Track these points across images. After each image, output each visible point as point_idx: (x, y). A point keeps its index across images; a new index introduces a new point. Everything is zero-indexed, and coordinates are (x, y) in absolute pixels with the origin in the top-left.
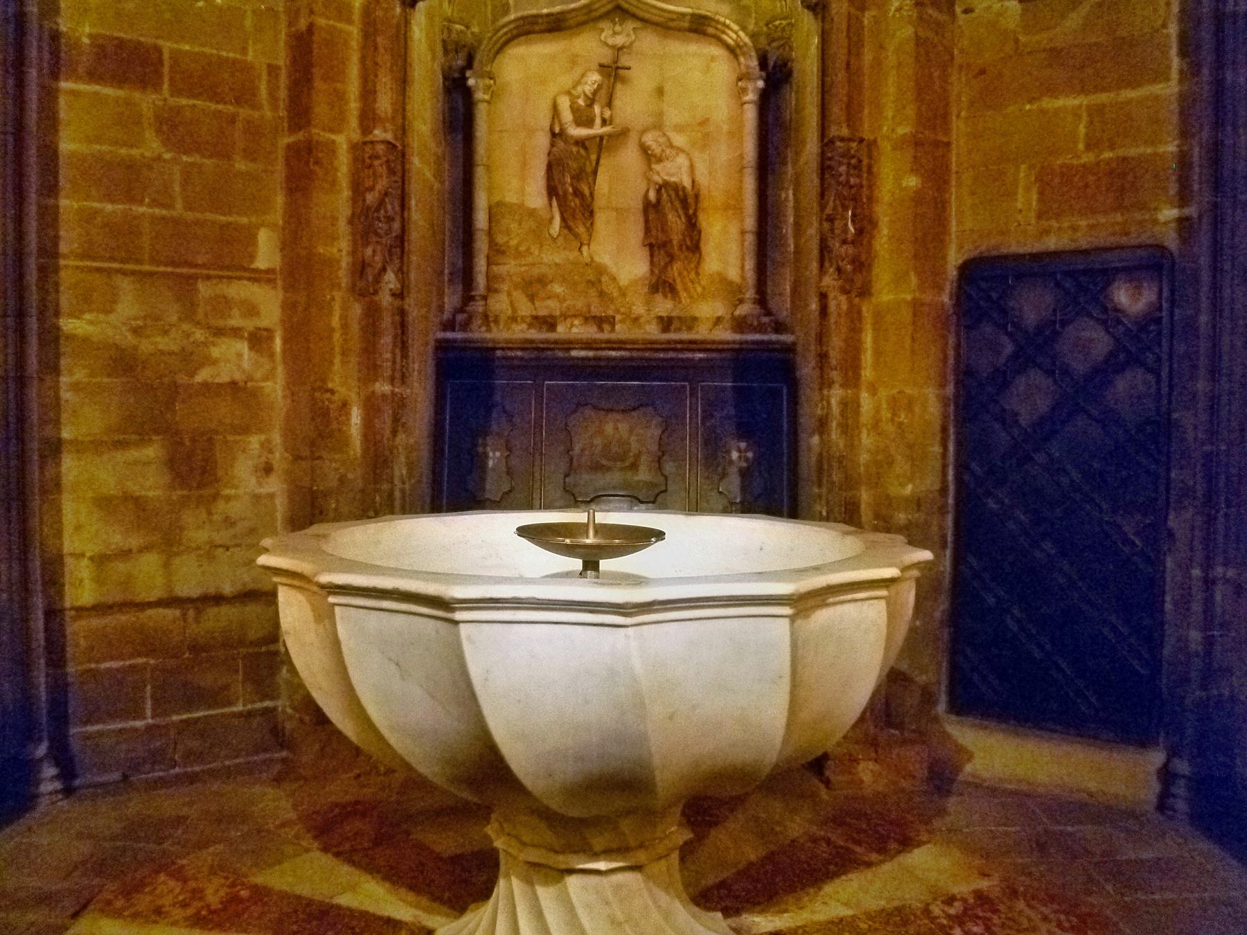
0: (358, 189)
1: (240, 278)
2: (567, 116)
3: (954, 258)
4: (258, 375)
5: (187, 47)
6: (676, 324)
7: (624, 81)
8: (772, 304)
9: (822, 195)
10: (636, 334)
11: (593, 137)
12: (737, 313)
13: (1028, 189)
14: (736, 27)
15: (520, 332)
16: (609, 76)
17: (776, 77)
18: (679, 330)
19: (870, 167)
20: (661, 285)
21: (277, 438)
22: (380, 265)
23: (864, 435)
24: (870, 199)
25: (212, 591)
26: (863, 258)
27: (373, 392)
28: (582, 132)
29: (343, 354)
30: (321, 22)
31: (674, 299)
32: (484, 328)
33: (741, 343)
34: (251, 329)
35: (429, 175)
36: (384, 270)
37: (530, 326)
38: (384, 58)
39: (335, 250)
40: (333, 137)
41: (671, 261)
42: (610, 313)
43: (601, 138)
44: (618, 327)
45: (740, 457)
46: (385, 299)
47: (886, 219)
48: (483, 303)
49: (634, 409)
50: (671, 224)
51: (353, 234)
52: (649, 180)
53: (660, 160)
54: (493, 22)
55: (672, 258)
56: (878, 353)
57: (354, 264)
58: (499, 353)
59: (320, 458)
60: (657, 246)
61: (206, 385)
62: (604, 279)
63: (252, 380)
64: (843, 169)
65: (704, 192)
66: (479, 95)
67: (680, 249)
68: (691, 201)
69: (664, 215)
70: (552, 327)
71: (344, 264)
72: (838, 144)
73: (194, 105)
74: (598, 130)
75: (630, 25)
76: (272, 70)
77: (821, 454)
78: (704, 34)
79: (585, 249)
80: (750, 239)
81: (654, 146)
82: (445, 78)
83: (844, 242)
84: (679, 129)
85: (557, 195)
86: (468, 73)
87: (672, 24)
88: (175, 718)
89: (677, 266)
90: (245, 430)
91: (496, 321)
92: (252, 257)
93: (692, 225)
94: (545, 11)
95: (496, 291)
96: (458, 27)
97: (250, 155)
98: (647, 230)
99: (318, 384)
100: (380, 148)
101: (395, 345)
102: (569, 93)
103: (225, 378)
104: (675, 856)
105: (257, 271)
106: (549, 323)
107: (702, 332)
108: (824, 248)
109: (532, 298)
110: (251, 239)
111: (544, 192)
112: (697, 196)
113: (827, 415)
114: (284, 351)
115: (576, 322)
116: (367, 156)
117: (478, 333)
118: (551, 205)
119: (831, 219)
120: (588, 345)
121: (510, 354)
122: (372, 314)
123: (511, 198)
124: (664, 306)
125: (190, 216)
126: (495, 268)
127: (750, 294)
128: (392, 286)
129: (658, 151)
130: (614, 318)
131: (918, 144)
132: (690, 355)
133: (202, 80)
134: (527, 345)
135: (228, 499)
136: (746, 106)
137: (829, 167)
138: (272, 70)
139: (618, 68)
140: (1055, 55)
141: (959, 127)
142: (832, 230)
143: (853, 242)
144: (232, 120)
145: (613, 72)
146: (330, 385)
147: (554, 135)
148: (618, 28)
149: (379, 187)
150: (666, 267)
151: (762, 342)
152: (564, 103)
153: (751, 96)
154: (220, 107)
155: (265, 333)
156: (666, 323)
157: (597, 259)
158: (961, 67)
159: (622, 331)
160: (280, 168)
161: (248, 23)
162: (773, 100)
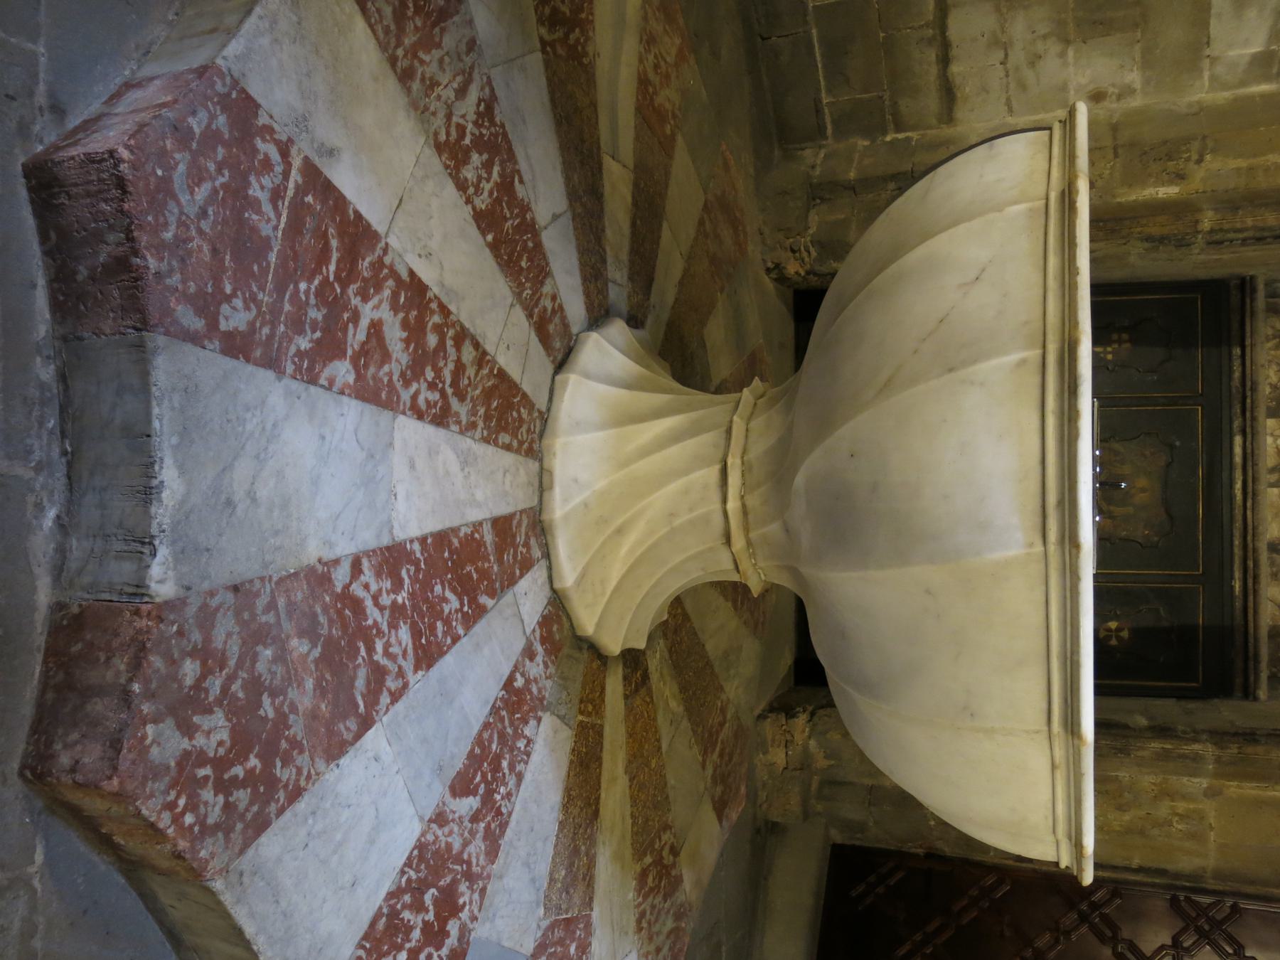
4: (1220, 70)
18: (1272, 563)
21: (1136, 102)
25: (954, 52)
27: (1200, 210)
32: (1270, 332)
33: (1256, 639)
45: (1110, 630)
59: (1116, 155)
63: (1212, 64)
77: (1126, 727)
88: (814, 31)
90: (1147, 63)
99: (1210, 144)
104: (736, 578)
113: (1177, 737)
114: (1250, 98)
120: (1250, 457)
132: (1237, 574)
134: (1248, 387)
135: (1062, 55)
146: (1208, 157)
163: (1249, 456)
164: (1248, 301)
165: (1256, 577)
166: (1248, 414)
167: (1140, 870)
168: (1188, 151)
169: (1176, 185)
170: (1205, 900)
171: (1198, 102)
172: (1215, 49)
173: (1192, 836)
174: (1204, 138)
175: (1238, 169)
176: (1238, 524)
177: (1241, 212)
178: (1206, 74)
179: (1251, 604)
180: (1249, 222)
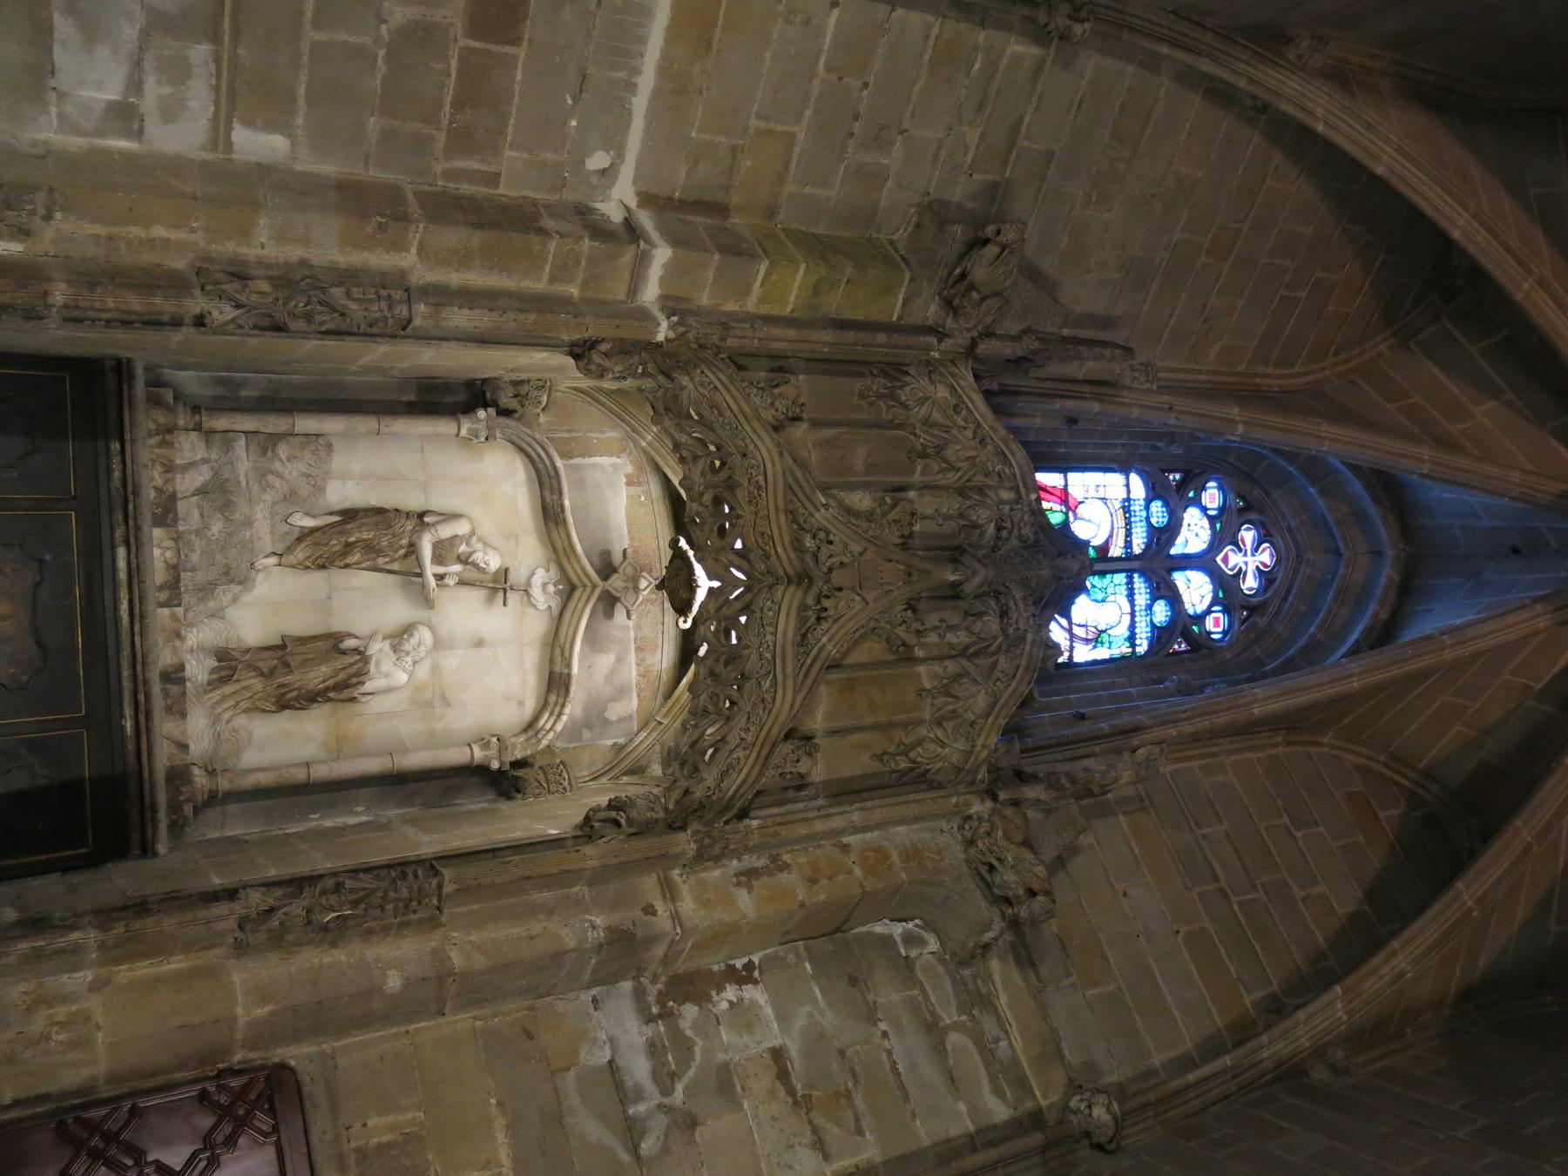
0: (349, 277)
1: (217, 103)
2: (445, 531)
3: (293, 1054)
4: (69, 108)
5: (519, 77)
6: (174, 689)
7: (490, 600)
8: (212, 814)
9: (368, 870)
10: (158, 638)
11: (419, 562)
12: (196, 771)
13: (392, 1128)
14: (559, 727)
15: (152, 479)
16: (494, 581)
17: (502, 780)
18: (166, 694)
19: (407, 924)
20: (228, 663)
22: (243, 299)
23: (22, 987)
24: (370, 932)
26: (289, 938)
27: (50, 280)
28: (427, 552)
29: (110, 238)
30: (552, 246)
31: (209, 683)
32: (152, 426)
33: (152, 785)
34: (142, 109)
35: (367, 359)
36: (238, 306)
37: (159, 491)
38: (510, 322)
39: (263, 240)
40: (414, 250)
41: (262, 674)
42: (186, 598)
43: (420, 575)
44: (166, 611)
46: (196, 304)
47: (343, 958)
48: (191, 426)
49: (39, 643)
50: (314, 671)
51: (287, 264)
52: (371, 637)
53: (395, 649)
54: (552, 440)
55: (269, 675)
56: (154, 983)
57: (246, 263)
58: (116, 446)
60: (283, 652)
61: (49, 29)
62: (236, 589)
64: (405, 893)
65: (357, 707)
66: (466, 426)
67: (283, 686)
68: (345, 694)
69: (324, 661)
70: (160, 521)
71: (243, 250)
72: (435, 882)
73: (449, 75)
74: (430, 570)
75: (555, 604)
76: (493, 179)
78: (549, 690)
79: (273, 560)
80: (301, 775)
81: (414, 641)
82: (484, 381)
83: (309, 911)
84: (436, 670)
85: (343, 522)
86: (492, 411)
87: (558, 651)
89: (257, 684)
91: (164, 444)
92: (249, 123)
93: (312, 698)
94: (567, 503)
95: (207, 442)
96: (545, 398)
97: (388, 136)
98: (302, 641)
100: (402, 310)
101: (129, 312)
102: (473, 533)
103: (60, 56)
105: (229, 129)
106: (167, 514)
107: (165, 727)
108: (298, 884)
109: (201, 491)
110: (271, 127)
111: (347, 505)
112: (352, 700)
114: (108, 153)
115: (169, 554)
116: (392, 292)
117: (145, 420)
118: (331, 514)
119: (338, 888)
120: (136, 572)
121: (116, 460)
122: (175, 284)
123: (337, 462)
124: (198, 670)
125: (305, 47)
126: (242, 442)
127: (224, 784)
128: (215, 314)
129: (407, 647)
130: (179, 605)
131: (441, 979)
132: (128, 711)
133: (480, 91)
136: (467, 750)
137: (404, 875)
138: (493, 179)
139: (505, 590)
140: (556, 1118)
141: (462, 1021)
142: (324, 892)
143: (309, 923)
144: (433, 121)
145: (499, 585)
146: (58, 215)
147: (421, 515)
148: (551, 589)
149: (353, 306)
150: (256, 669)
151: (154, 810)
152: (461, 528)
153: (479, 754)
154: (447, 108)
155: (136, 127)
156: (174, 676)
157: (260, 577)
158: (532, 1008)
159: (161, 616)
160: (375, 174)
161: (549, 156)
162: (474, 779)
163: (134, 572)
164: (125, 387)
165: (148, 714)
166: (131, 522)
167: (16, 1103)
168: (31, 202)
169: (20, 241)
170: (97, 1113)
171: (45, 143)
172: (62, 81)
173: (75, 1044)
174: (51, 190)
175: (98, 236)
176: (126, 652)
177: (99, 290)
178: (53, 110)
179: (144, 746)
180: (110, 302)
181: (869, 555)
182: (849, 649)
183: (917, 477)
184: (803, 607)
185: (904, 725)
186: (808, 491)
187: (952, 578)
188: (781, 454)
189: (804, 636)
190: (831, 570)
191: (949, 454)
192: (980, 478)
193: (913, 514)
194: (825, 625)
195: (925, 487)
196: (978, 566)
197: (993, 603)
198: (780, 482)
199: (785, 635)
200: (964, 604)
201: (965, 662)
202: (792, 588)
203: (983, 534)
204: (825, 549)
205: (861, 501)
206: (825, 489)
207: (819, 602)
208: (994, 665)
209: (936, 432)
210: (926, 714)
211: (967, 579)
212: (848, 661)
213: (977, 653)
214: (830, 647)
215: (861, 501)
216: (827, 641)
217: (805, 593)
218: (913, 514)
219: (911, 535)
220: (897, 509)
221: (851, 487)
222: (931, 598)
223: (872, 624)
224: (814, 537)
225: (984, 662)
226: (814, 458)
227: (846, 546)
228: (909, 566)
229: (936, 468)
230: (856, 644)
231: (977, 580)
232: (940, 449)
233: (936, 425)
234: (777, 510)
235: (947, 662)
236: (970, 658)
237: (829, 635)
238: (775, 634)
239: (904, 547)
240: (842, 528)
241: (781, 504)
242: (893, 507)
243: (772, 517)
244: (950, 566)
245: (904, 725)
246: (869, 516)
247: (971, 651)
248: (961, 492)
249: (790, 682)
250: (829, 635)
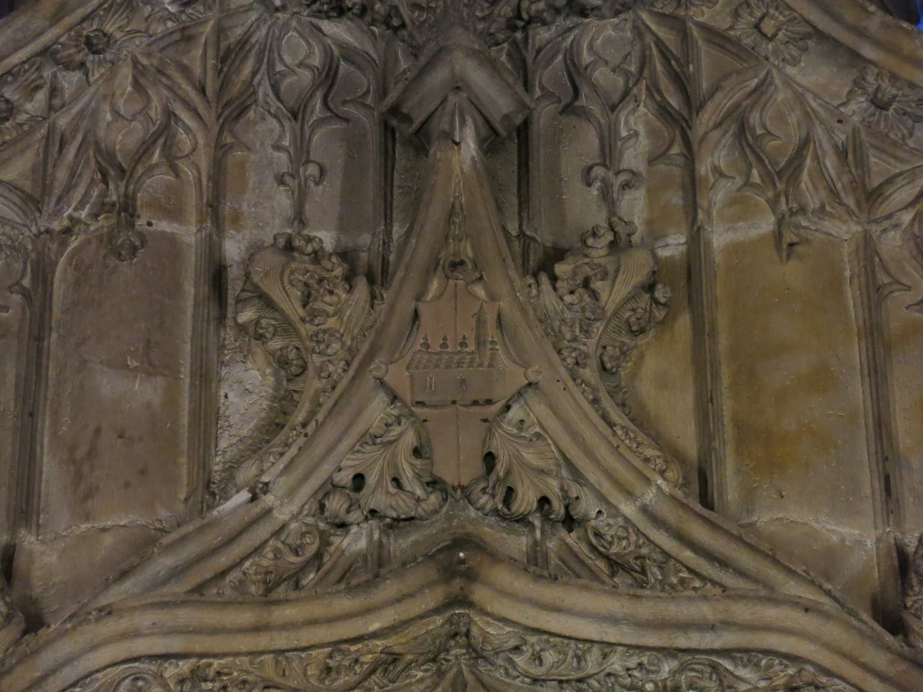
181: (398, 376)
182: (657, 440)
183: (188, 233)
184: (534, 563)
185: (875, 295)
186: (212, 538)
187: (470, 147)
188: (108, 612)
189: (615, 565)
190: (434, 483)
191: (123, 138)
192: (196, 58)
193: (289, 247)
194: (588, 506)
195: (215, 212)
196: (439, 76)
197: (542, 35)
198: (186, 616)
199: (613, 620)
200: (544, 115)
201: (705, 120)
202: (480, 594)
203: (348, 53)
204: (378, 497)
205: (245, 391)
206: (210, 491)
207: (523, 520)
208: (718, 38)
209: (62, 174)
210: (845, 230)
211: (477, 106)
212: (690, 445)
213: (681, 82)
214: (649, 496)
215: (245, 391)
216: (632, 500)
217: (494, 557)
218: (289, 247)
219: (345, 255)
220: (277, 295)
221: (207, 417)
222: (524, 201)
223: (589, 373)
224: (343, 526)
225: (706, 63)
226: (120, 519)
227: (370, 439)
228: (433, 266)
229: (162, 178)
230: (641, 420)
231: (478, 77)
232: (110, 167)
233: (42, 172)
234: (257, 629)
235: (704, 168)
236: (693, 104)
237: (615, 497)
238: (608, 647)
239: (378, 277)
240: (319, 448)
241: (246, 617)
242: (268, 303)
243: (281, 641)
244: (437, 151)
245: (875, 295)
246: (290, 370)
247: (674, 101)
248: (233, 110)
249: (742, 611)
250: (615, 497)
